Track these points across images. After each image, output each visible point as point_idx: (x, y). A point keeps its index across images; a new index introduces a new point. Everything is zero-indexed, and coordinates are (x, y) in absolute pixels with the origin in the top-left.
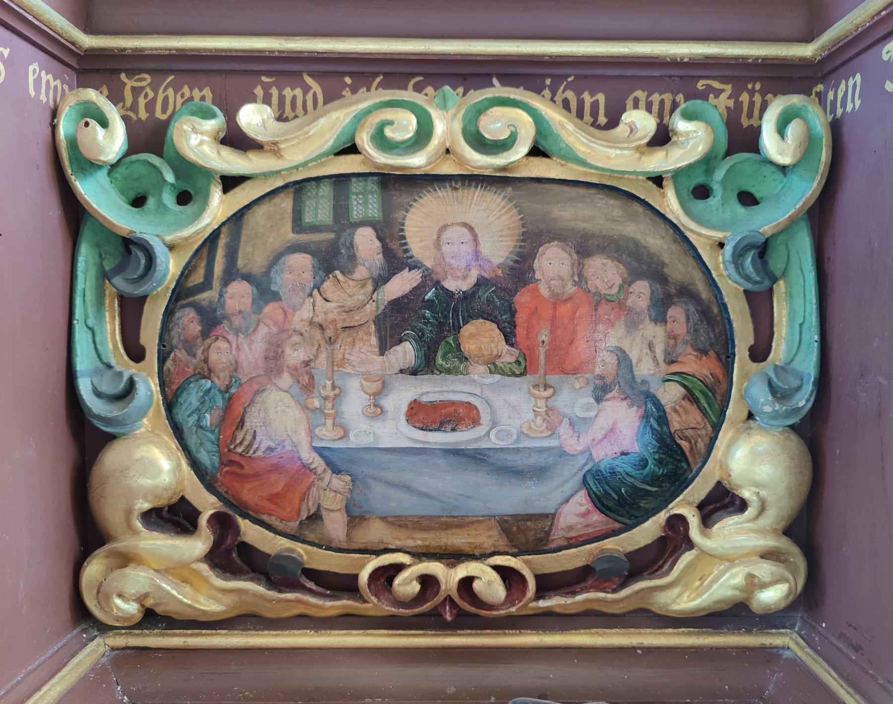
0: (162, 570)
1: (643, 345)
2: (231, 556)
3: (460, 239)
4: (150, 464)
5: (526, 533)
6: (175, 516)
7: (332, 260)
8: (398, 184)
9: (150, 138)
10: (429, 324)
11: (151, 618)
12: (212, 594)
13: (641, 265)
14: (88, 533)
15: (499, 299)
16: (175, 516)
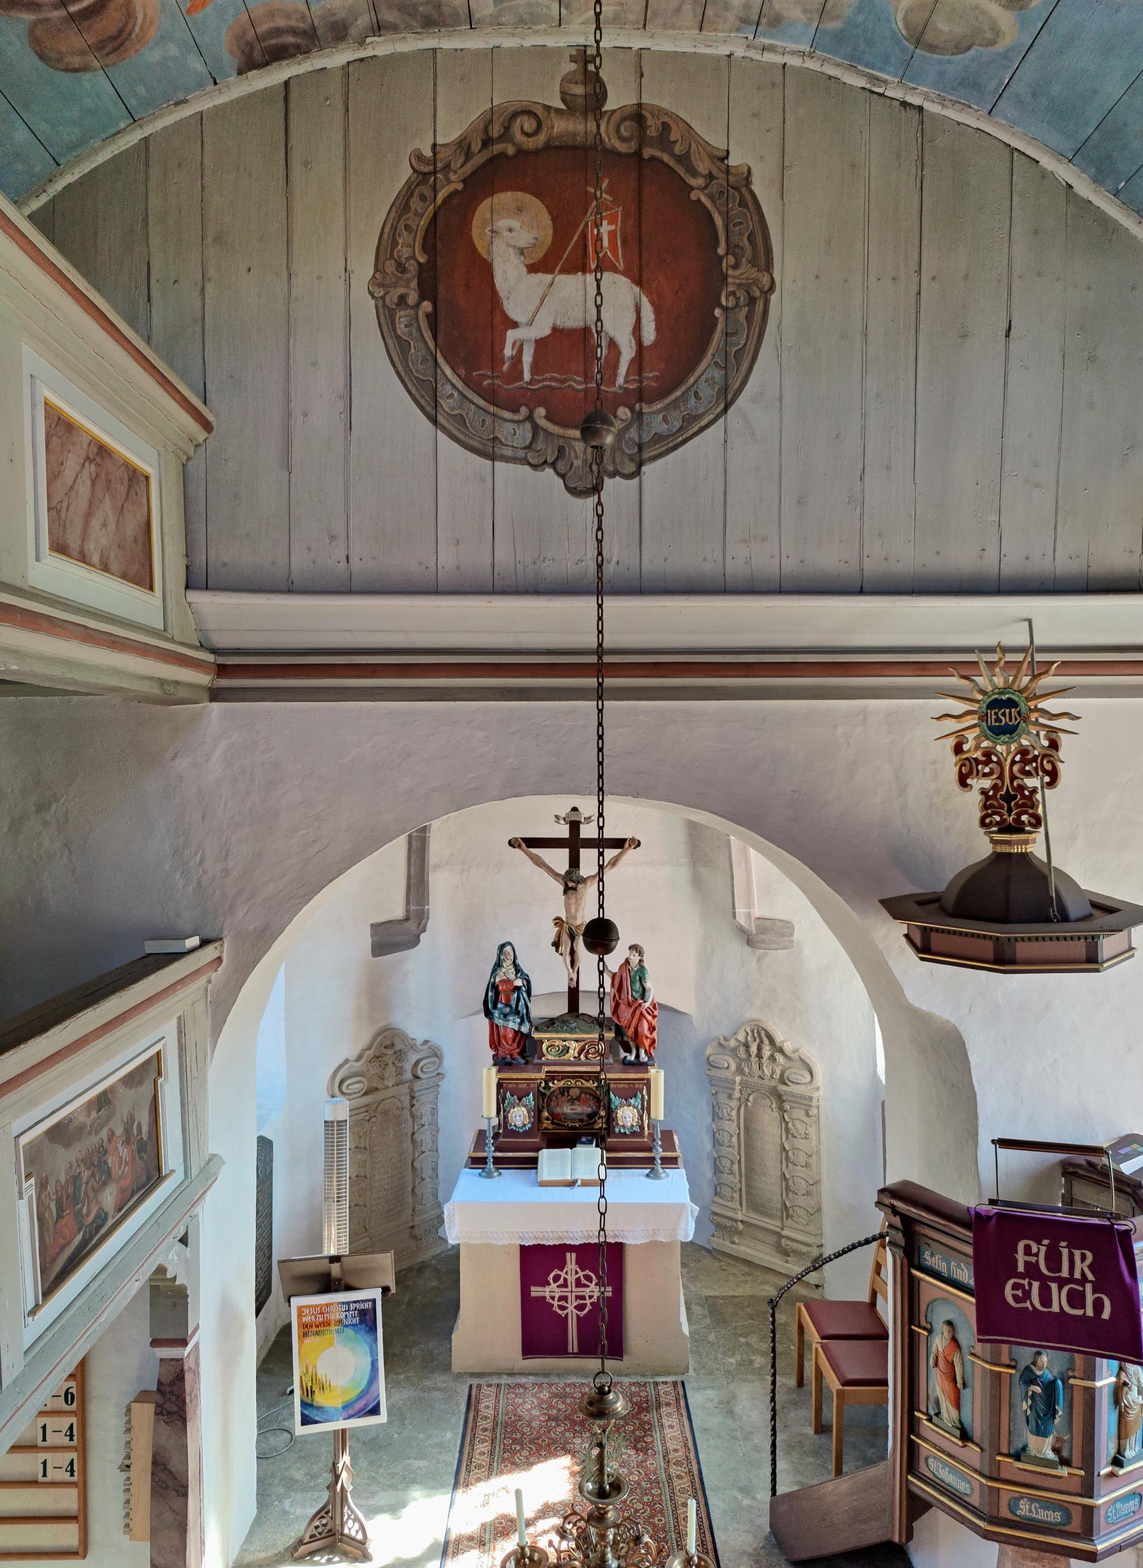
0: (547, 1124)
1: (592, 1103)
2: (553, 1123)
3: (575, 1093)
4: (546, 1114)
5: (581, 1120)
6: (547, 1119)
7: (563, 1095)
8: (569, 1088)
9: (546, 1083)
10: (572, 1101)
11: (546, 1129)
12: (551, 1127)
13: (590, 1094)
14: (540, 1121)
15: (578, 1099)
16: (547, 1119)
